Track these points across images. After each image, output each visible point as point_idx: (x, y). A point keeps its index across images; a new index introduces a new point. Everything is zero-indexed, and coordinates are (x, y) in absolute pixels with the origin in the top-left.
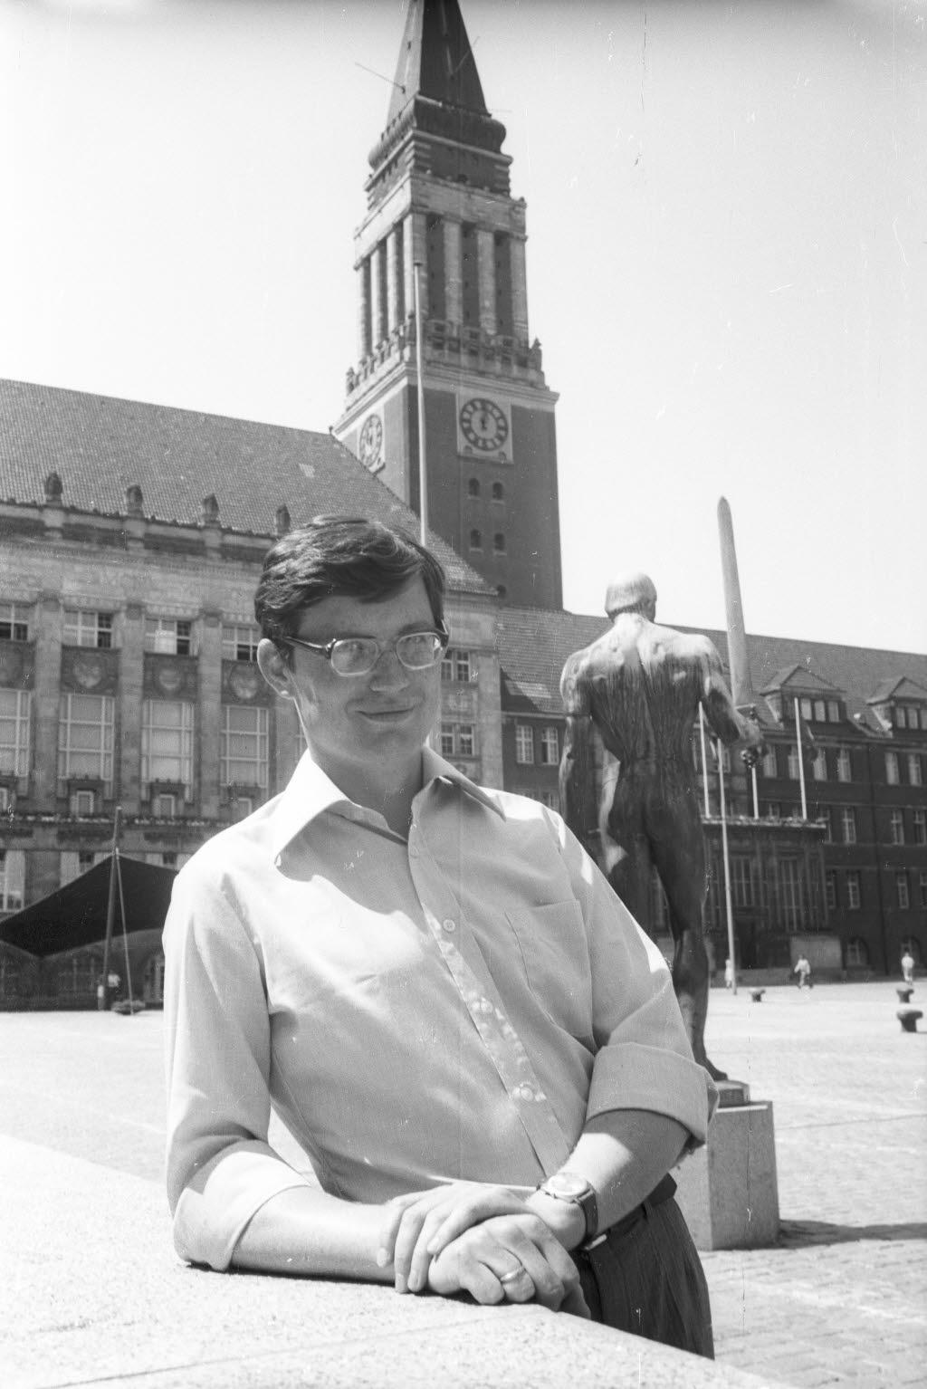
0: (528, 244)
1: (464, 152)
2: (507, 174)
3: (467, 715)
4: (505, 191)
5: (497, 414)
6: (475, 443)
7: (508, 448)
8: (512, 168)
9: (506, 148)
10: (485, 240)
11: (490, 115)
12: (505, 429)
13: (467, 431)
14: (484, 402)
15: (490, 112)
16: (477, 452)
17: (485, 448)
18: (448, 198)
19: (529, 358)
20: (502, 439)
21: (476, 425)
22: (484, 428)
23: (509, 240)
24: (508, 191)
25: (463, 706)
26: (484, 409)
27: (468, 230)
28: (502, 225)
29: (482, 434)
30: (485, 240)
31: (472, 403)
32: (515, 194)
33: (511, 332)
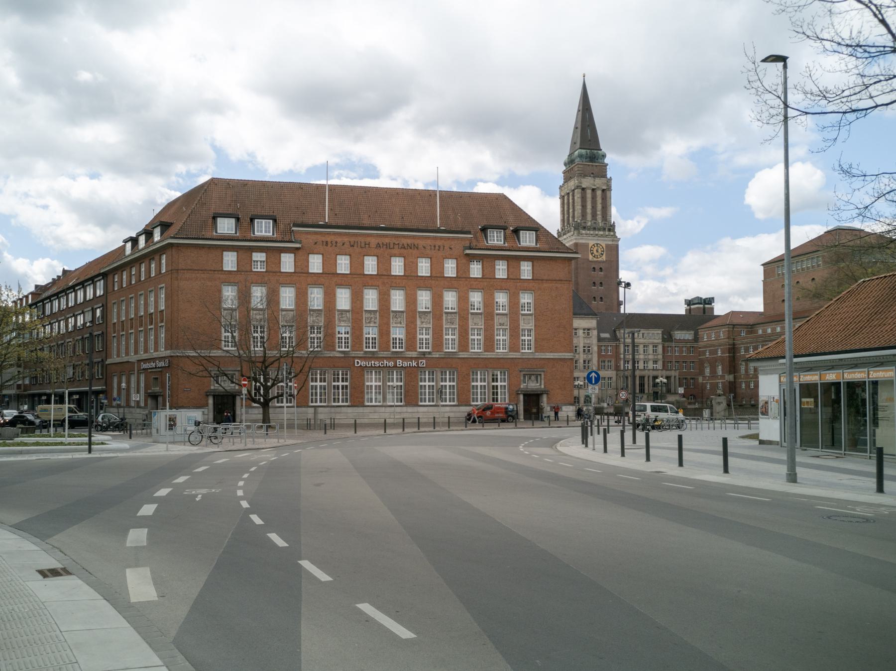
0: (612, 192)
1: (592, 165)
2: (606, 169)
3: (589, 344)
4: (605, 176)
5: (601, 247)
6: (594, 257)
7: (604, 258)
8: (608, 167)
9: (606, 161)
10: (599, 193)
11: (601, 150)
12: (603, 251)
13: (592, 254)
14: (597, 244)
15: (601, 148)
16: (595, 259)
17: (597, 258)
18: (587, 182)
19: (611, 228)
20: (602, 254)
21: (595, 252)
22: (597, 251)
23: (606, 192)
24: (606, 175)
25: (589, 342)
26: (597, 246)
27: (593, 190)
28: (604, 188)
29: (596, 254)
30: (599, 193)
31: (594, 245)
32: (608, 176)
33: (606, 220)
